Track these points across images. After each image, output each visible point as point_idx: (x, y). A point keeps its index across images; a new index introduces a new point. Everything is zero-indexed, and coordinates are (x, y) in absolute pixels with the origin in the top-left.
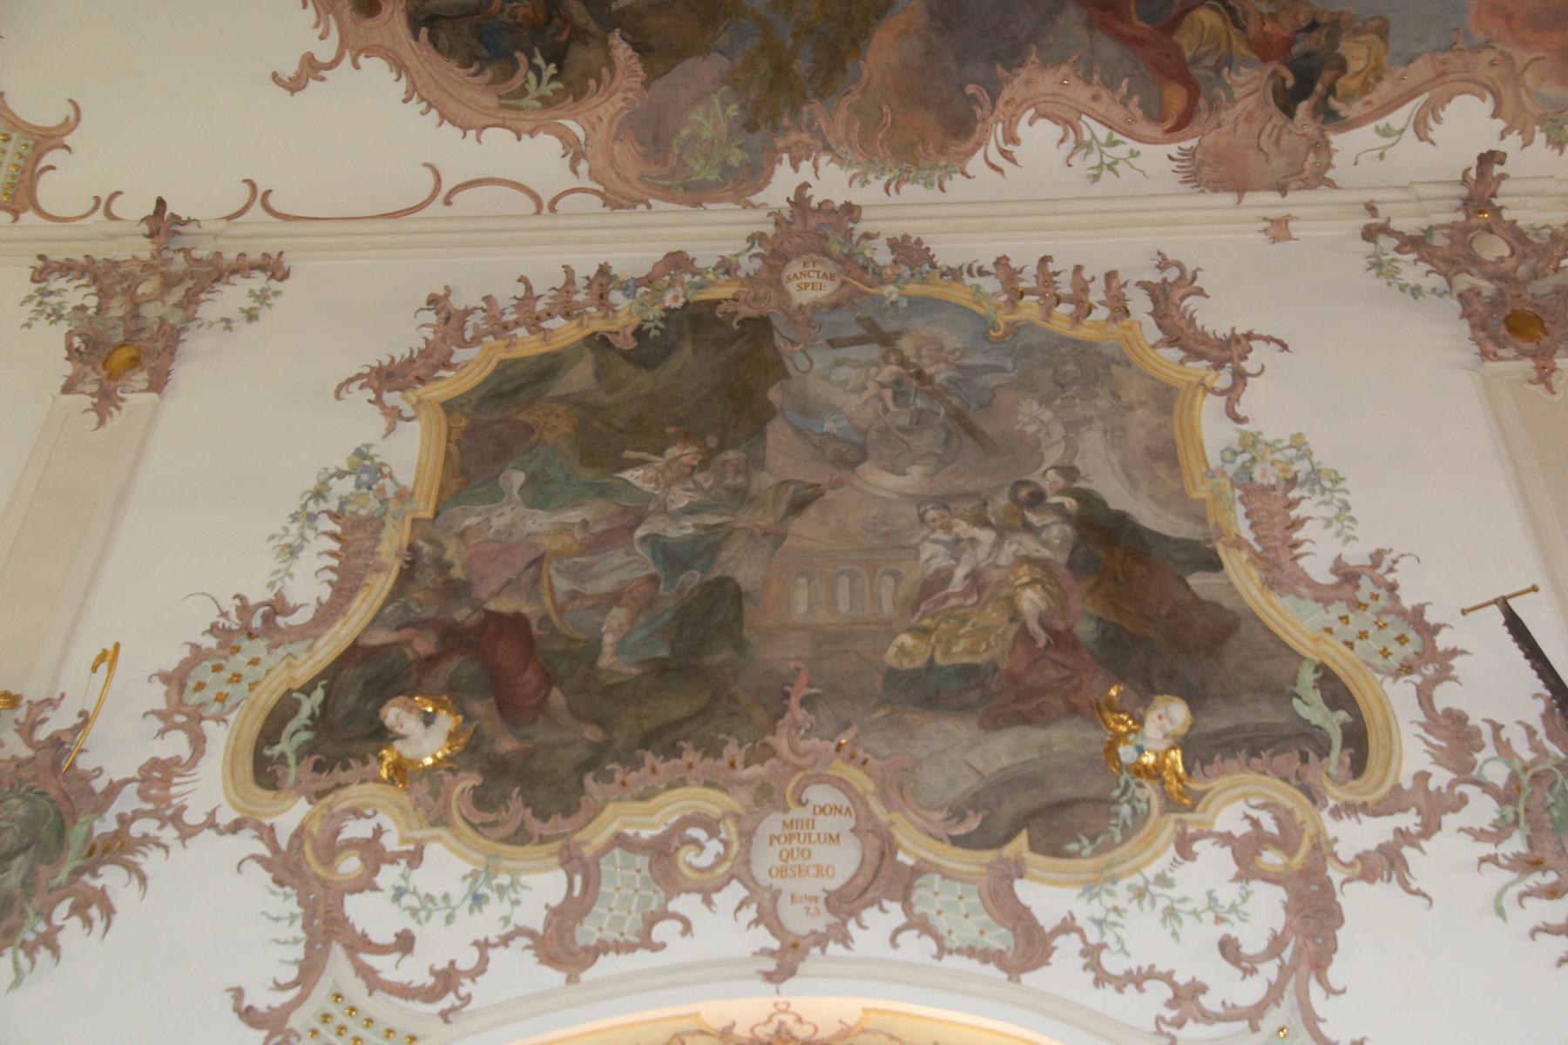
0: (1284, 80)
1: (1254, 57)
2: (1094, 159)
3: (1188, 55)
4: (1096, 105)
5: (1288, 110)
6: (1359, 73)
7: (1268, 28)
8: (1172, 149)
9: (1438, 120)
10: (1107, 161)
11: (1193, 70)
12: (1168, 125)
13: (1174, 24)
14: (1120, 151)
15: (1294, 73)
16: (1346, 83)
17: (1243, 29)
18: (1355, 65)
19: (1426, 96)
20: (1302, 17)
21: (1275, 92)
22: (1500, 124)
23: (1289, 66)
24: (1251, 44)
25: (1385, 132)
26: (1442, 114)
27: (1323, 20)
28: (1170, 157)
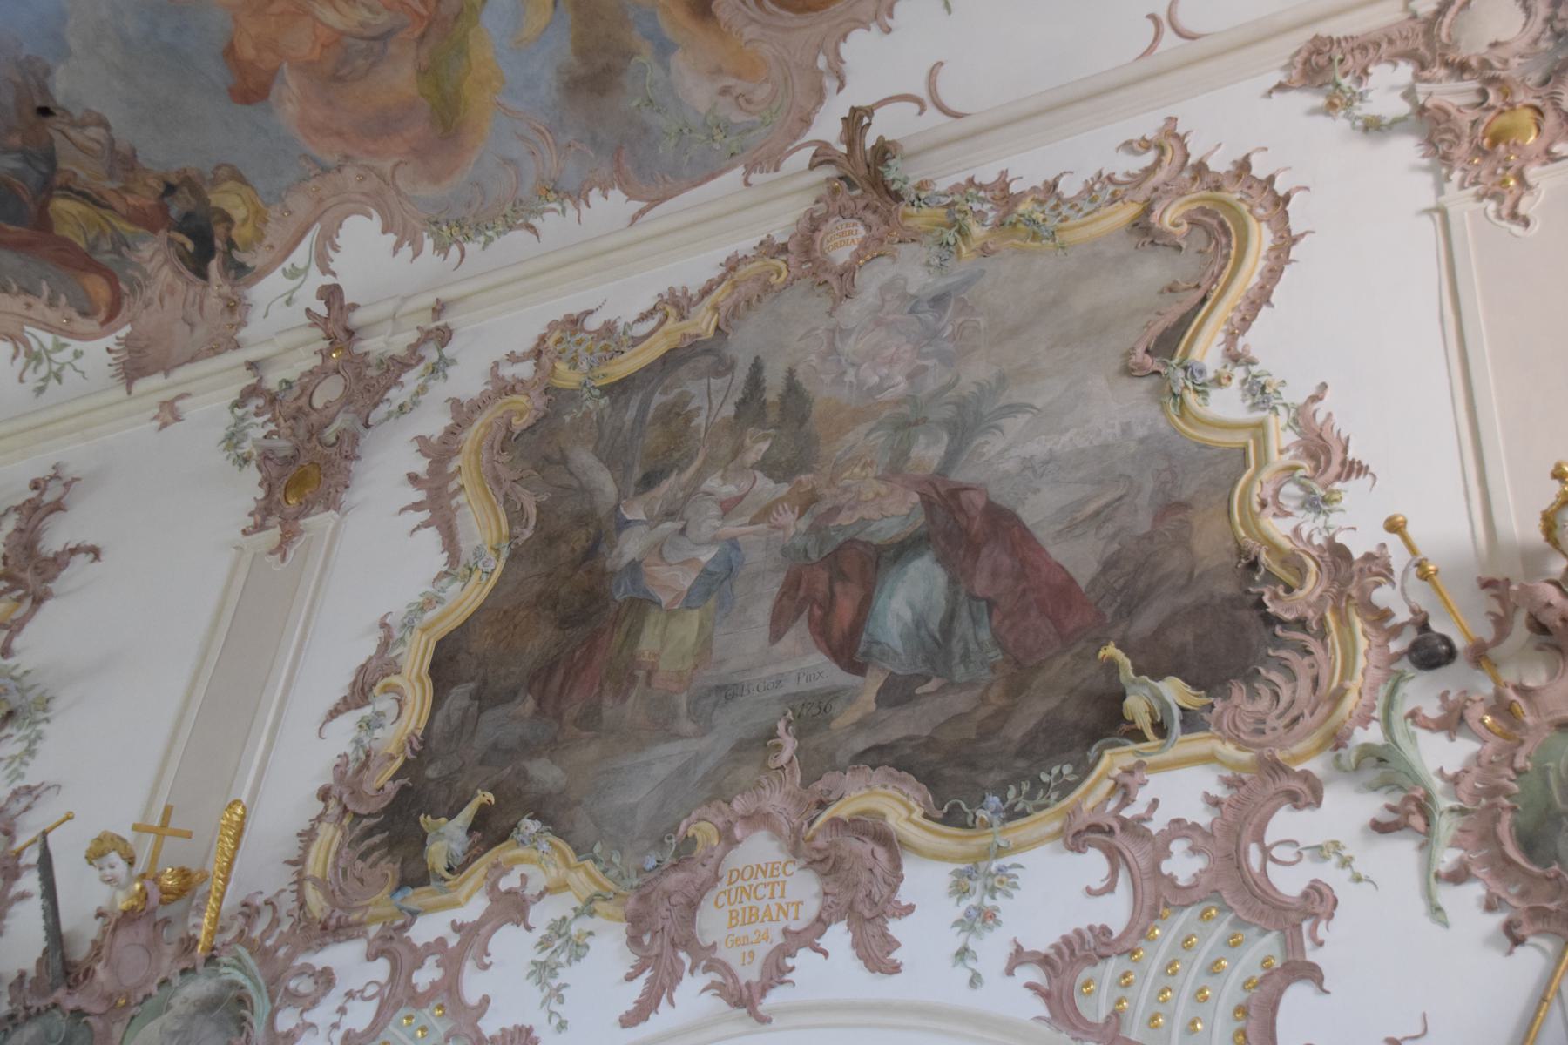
0: (183, 245)
1: (141, 230)
2: (43, 370)
3: (82, 244)
4: (31, 313)
5: (202, 274)
6: (245, 221)
7: (131, 200)
8: (110, 341)
9: (336, 248)
10: (55, 367)
11: (97, 257)
12: (102, 316)
13: (43, 222)
14: (64, 356)
15: (190, 235)
16: (240, 233)
17: (110, 207)
18: (238, 213)
19: (317, 226)
20: (152, 182)
21: (182, 258)
22: (392, 238)
23: (180, 230)
24: (129, 219)
25: (293, 273)
26: (337, 241)
27: (174, 180)
28: (109, 350)
